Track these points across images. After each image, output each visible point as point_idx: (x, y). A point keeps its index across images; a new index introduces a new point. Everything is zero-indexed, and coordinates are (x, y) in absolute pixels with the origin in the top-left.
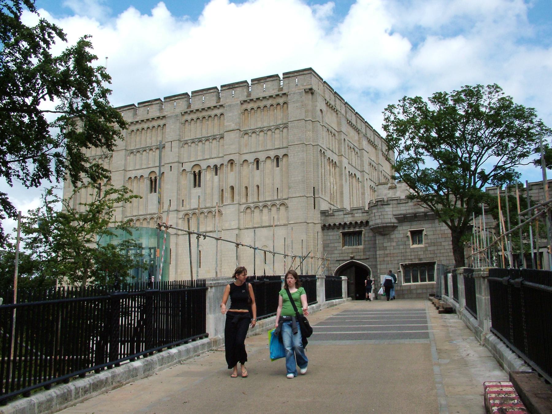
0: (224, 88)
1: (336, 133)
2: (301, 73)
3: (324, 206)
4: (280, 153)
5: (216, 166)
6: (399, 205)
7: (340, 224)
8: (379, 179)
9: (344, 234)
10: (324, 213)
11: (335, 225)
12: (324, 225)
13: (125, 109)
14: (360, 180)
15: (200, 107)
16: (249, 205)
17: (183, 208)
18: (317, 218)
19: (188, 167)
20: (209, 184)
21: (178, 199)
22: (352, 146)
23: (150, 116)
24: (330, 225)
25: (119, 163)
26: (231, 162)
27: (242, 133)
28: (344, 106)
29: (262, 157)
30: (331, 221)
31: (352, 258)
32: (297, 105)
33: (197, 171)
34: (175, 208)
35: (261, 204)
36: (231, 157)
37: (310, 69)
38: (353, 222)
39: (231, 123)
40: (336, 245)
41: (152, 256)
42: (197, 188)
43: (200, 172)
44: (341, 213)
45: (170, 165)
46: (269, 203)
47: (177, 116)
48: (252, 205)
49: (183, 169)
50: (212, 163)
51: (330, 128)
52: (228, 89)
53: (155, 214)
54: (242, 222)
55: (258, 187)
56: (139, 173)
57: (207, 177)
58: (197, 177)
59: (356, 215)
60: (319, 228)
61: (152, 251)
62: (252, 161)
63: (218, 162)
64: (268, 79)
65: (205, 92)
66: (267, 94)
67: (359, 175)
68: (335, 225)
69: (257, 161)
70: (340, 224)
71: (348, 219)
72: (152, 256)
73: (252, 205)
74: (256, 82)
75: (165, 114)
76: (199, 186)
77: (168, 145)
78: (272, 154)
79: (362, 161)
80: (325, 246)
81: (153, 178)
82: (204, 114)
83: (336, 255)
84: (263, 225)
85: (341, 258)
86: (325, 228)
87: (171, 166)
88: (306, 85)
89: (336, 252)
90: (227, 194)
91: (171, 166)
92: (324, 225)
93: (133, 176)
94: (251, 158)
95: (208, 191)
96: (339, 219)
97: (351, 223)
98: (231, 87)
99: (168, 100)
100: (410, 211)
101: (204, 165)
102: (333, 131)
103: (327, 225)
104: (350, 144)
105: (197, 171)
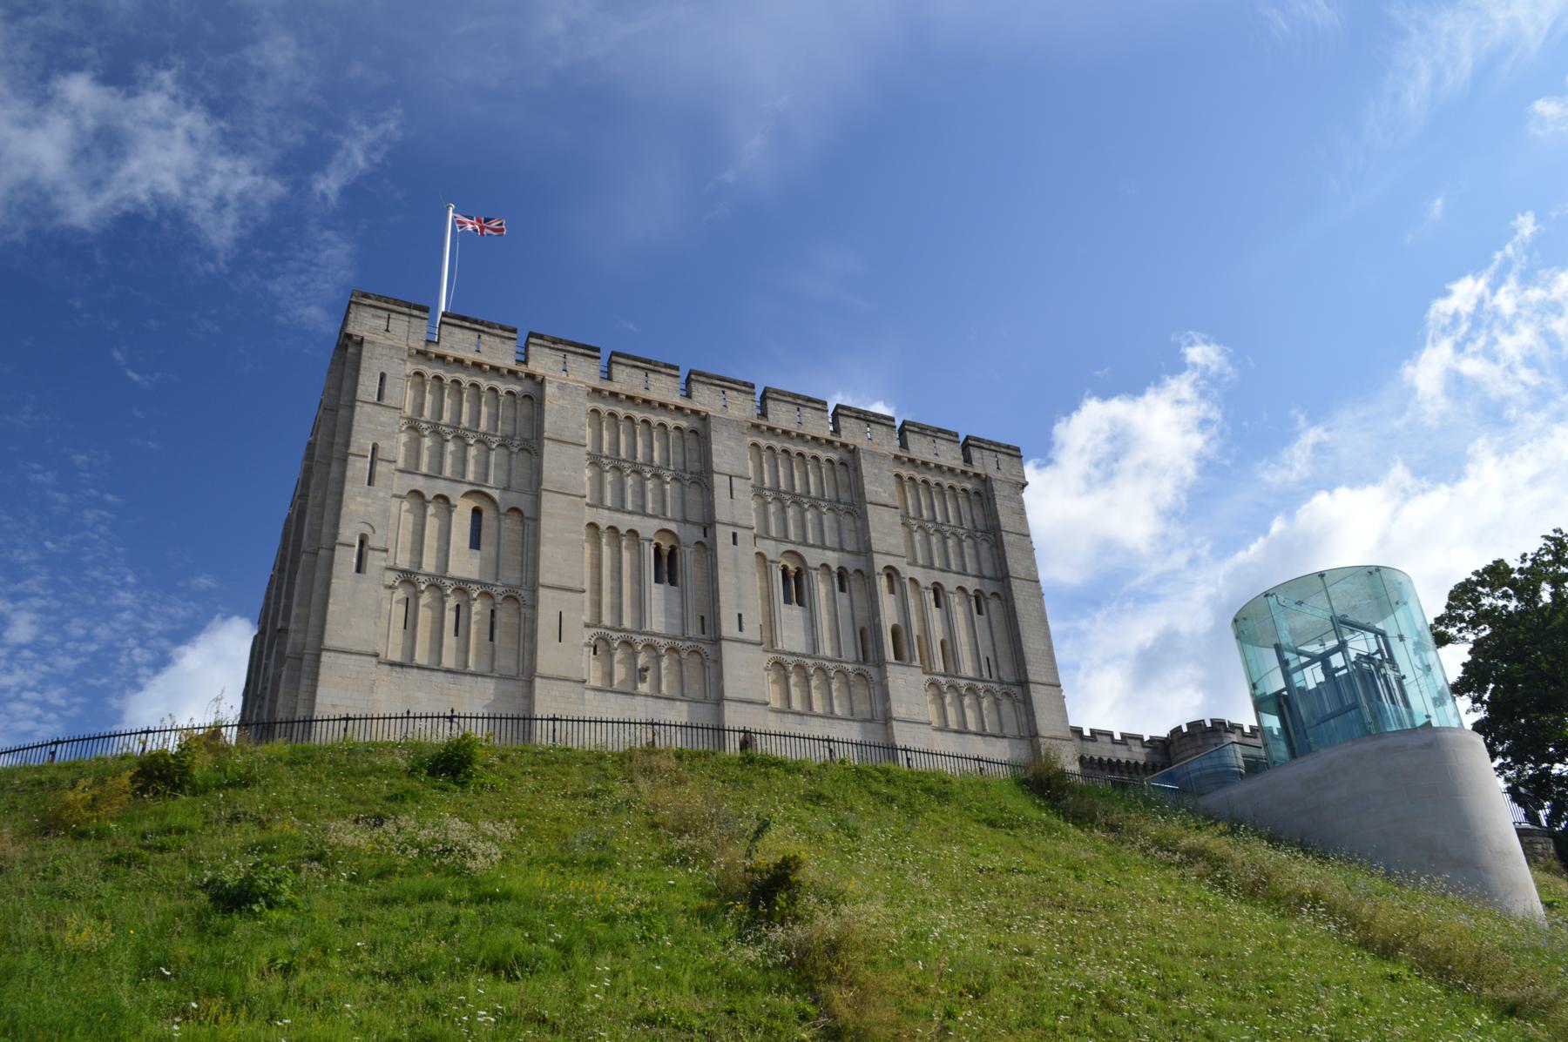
13: (572, 349)
15: (792, 427)
16: (938, 678)
23: (653, 395)
25: (565, 473)
26: (891, 573)
29: (950, 582)
33: (791, 567)
36: (891, 561)
37: (1018, 450)
39: (880, 490)
45: (731, 530)
48: (943, 680)
49: (756, 550)
52: (857, 418)
56: (625, 522)
57: (821, 589)
59: (1134, 749)
62: (930, 586)
64: (940, 435)
69: (937, 589)
71: (1122, 754)
73: (943, 680)
74: (916, 429)
77: (720, 483)
81: (665, 547)
87: (734, 535)
88: (1015, 476)
91: (734, 535)
93: (603, 524)
94: (925, 578)
101: (813, 557)
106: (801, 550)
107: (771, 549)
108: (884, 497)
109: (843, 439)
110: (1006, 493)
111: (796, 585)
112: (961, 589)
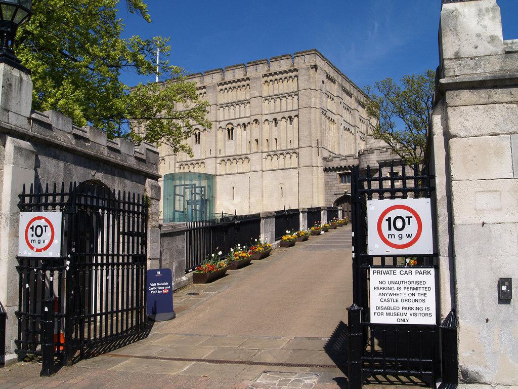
0: (249, 65)
1: (334, 98)
2: (308, 53)
3: (326, 154)
4: (293, 114)
5: (244, 124)
6: (381, 154)
7: (337, 167)
8: (367, 131)
9: (340, 175)
10: (325, 159)
11: (333, 167)
12: (326, 168)
14: (352, 133)
17: (220, 156)
18: (319, 161)
19: (223, 124)
20: (238, 137)
21: (216, 149)
22: (347, 107)
24: (329, 168)
26: (256, 121)
27: (263, 99)
28: (340, 76)
29: (279, 117)
30: (330, 165)
31: (346, 192)
32: (306, 77)
33: (230, 128)
34: (214, 156)
35: (278, 152)
36: (256, 117)
38: (347, 166)
40: (334, 182)
41: (203, 193)
42: (231, 140)
43: (232, 129)
44: (338, 159)
46: (284, 152)
47: (214, 86)
50: (241, 121)
51: (330, 95)
53: (199, 160)
54: (264, 166)
55: (276, 139)
57: (238, 131)
58: (231, 132)
60: (321, 170)
61: (203, 189)
63: (246, 121)
65: (234, 68)
66: (282, 69)
67: (352, 129)
68: (333, 167)
69: (275, 120)
70: (337, 167)
71: (343, 164)
72: (203, 193)
73: (272, 153)
74: (274, 60)
75: (205, 84)
76: (232, 139)
78: (287, 115)
79: (355, 118)
80: (327, 184)
81: (197, 132)
82: (234, 84)
83: (335, 191)
84: (280, 168)
85: (338, 193)
86: (326, 170)
89: (334, 188)
90: (254, 144)
92: (326, 168)
94: (270, 118)
95: (238, 142)
96: (336, 163)
97: (345, 167)
98: (255, 64)
99: (207, 74)
100: (389, 158)
101: (235, 123)
102: (332, 96)
103: (327, 168)
104: (345, 105)
105: (230, 128)
106: (232, 121)
107: (223, 124)
108: (257, 94)
109: (247, 77)
110: (302, 74)
111: (230, 133)
112: (284, 118)
